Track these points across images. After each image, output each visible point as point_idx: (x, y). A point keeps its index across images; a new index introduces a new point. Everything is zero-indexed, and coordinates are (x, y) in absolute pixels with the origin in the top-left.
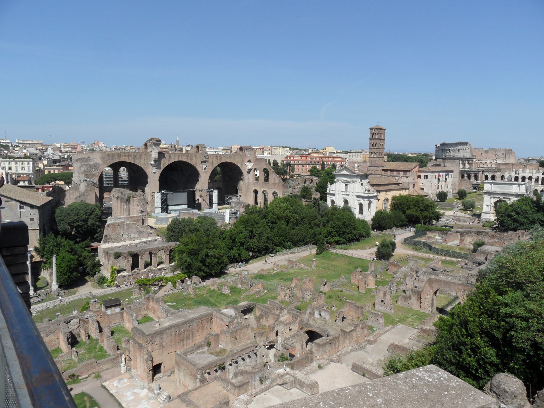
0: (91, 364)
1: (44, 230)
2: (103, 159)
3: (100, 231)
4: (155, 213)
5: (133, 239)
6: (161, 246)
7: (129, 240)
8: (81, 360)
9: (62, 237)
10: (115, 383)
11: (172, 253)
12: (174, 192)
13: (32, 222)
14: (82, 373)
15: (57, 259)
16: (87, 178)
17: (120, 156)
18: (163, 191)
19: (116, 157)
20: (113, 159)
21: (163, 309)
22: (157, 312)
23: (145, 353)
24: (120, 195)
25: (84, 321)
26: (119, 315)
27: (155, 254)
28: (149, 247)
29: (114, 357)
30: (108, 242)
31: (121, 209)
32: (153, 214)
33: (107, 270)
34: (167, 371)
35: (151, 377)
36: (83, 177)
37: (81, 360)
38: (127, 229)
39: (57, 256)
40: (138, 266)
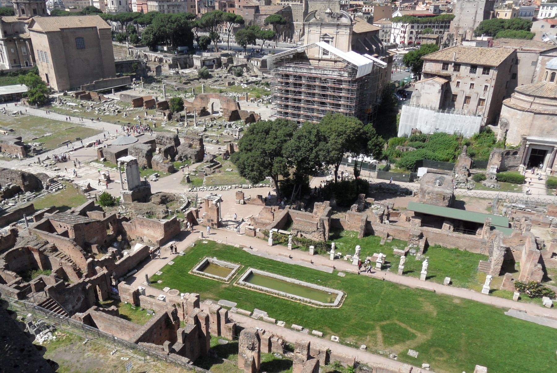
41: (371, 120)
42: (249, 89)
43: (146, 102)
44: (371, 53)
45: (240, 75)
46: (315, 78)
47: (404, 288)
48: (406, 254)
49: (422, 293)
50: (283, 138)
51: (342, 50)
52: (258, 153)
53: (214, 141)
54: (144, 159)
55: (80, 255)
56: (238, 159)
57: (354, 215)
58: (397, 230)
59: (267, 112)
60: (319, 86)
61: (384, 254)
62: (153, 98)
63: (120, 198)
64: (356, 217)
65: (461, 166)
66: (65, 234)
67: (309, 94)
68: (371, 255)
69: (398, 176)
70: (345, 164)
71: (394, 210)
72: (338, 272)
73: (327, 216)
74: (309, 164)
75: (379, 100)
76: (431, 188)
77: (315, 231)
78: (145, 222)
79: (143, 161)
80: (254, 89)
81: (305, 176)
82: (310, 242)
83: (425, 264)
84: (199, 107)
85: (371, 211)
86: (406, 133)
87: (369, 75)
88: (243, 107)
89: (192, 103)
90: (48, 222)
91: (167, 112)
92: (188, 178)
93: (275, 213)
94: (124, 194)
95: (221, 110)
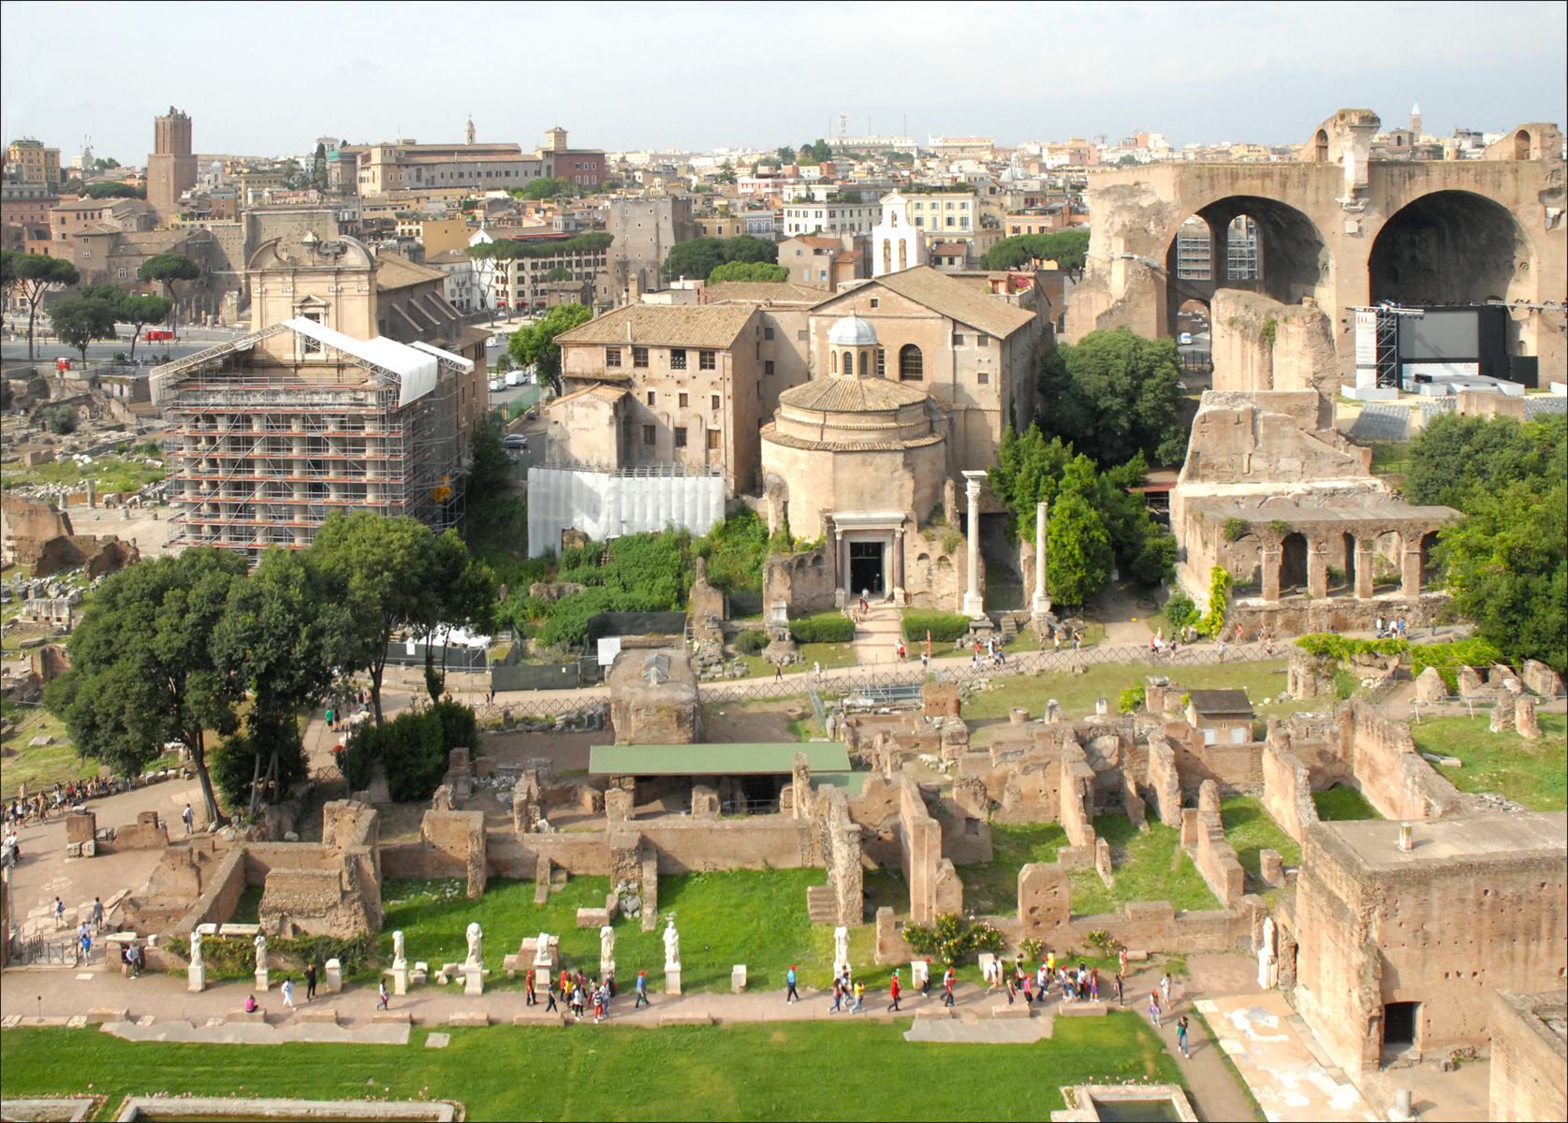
0: (1159, 915)
1: (1013, 413)
2: (1181, 186)
3: (1177, 433)
4: (1353, 385)
5: (1284, 475)
6: (1390, 513)
7: (1274, 476)
8: (1124, 891)
9: (1064, 444)
10: (1240, 1017)
11: (1434, 550)
12: (1426, 310)
13: (983, 386)
14: (1128, 939)
15: (1049, 515)
16: (1133, 250)
17: (1234, 176)
18: (1384, 307)
19: (1223, 182)
20: (1212, 187)
21: (1410, 772)
22: (1385, 781)
23: (1355, 941)
24: (1241, 311)
25: (1134, 752)
26: (1247, 756)
27: (1368, 545)
28: (1344, 516)
29: (1233, 914)
30: (1203, 477)
31: (1243, 366)
32: (1347, 391)
33: (1200, 577)
34: (1439, 1044)
35: (1374, 1049)
36: (1119, 247)
37: (1124, 891)
38: (1267, 437)
39: (1051, 503)
40: (1303, 582)
42: (97, 469)
44: (428, 337)
45: (67, 428)
46: (288, 418)
47: (629, 1037)
48: (617, 918)
49: (685, 1038)
50: (208, 609)
51: (354, 335)
52: (133, 668)
56: (70, 698)
57: (446, 822)
58: (576, 844)
59: (155, 534)
60: (302, 440)
61: (552, 933)
64: (453, 827)
67: (276, 463)
68: (514, 947)
69: (548, 675)
70: (398, 663)
73: (365, 843)
74: (291, 678)
80: (115, 468)
81: (287, 720)
82: (327, 947)
83: (670, 937)
85: (494, 799)
87: (431, 394)
88: (81, 525)
95: (10, 543)
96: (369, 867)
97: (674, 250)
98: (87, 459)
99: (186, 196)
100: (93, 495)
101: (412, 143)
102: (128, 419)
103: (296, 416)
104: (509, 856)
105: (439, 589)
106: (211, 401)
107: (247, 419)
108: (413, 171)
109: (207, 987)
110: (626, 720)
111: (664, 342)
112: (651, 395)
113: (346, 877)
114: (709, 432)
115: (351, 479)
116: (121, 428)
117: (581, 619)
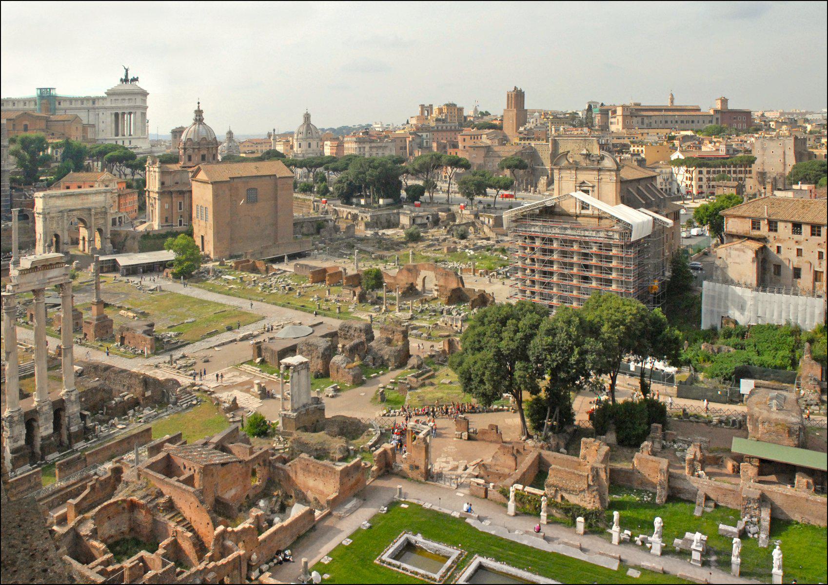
41: (658, 303)
42: (476, 257)
43: (330, 275)
44: (648, 206)
45: (463, 237)
46: (572, 242)
50: (528, 331)
51: (607, 202)
53: (425, 335)
54: (320, 361)
55: (207, 518)
57: (647, 461)
58: (721, 489)
59: (503, 292)
60: (579, 253)
61: (703, 534)
62: (341, 269)
63: (277, 423)
64: (650, 464)
65: (807, 377)
66: (189, 481)
67: (565, 264)
68: (681, 536)
70: (625, 374)
71: (712, 451)
72: (627, 568)
73: (602, 462)
74: (568, 372)
75: (668, 274)
76: (765, 414)
77: (584, 491)
78: (311, 467)
79: (317, 365)
80: (485, 258)
81: (565, 393)
84: (405, 282)
86: (714, 323)
87: (649, 236)
88: (469, 283)
89: (395, 278)
90: (168, 458)
91: (358, 290)
92: (382, 393)
93: (518, 456)
94: (285, 418)
96: (603, 475)
97: (794, 167)
98: (472, 252)
99: (521, 129)
100: (474, 270)
101: (639, 105)
102: (492, 235)
103: (576, 241)
104: (681, 486)
105: (649, 339)
106: (533, 230)
107: (551, 240)
108: (639, 119)
109: (516, 515)
110: (756, 428)
111: (788, 219)
112: (779, 248)
113: (590, 478)
114: (816, 272)
115: (604, 276)
116: (488, 239)
117: (731, 367)
